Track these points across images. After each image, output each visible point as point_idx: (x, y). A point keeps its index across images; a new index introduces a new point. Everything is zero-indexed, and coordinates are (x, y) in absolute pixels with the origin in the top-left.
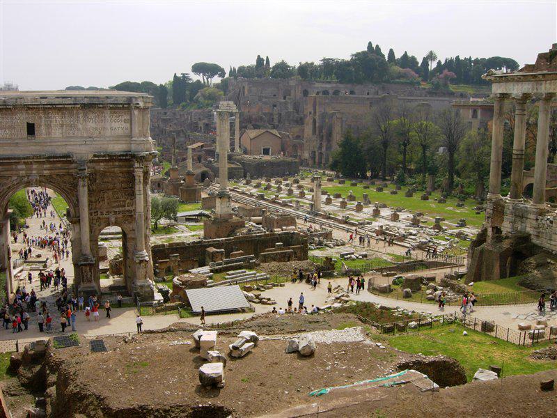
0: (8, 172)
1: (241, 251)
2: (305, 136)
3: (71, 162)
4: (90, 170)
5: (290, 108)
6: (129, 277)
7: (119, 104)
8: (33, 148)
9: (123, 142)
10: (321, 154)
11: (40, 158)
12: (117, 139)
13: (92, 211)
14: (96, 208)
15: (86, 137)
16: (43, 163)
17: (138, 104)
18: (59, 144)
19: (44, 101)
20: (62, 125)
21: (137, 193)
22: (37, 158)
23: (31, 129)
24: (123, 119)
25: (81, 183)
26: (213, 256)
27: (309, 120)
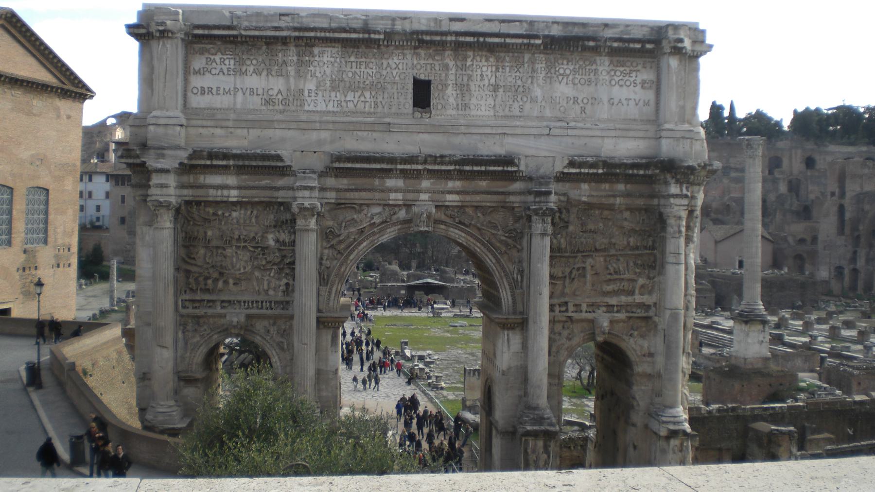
0: (364, 195)
2: (821, 237)
3: (511, 177)
4: (556, 197)
5: (783, 188)
9: (641, 134)
10: (855, 271)
11: (442, 163)
14: (563, 294)
15: (550, 119)
17: (681, 41)
18: (488, 130)
19: (457, 27)
20: (496, 88)
21: (670, 259)
22: (435, 163)
24: (639, 80)
25: (538, 226)
26: (770, 441)
27: (830, 206)
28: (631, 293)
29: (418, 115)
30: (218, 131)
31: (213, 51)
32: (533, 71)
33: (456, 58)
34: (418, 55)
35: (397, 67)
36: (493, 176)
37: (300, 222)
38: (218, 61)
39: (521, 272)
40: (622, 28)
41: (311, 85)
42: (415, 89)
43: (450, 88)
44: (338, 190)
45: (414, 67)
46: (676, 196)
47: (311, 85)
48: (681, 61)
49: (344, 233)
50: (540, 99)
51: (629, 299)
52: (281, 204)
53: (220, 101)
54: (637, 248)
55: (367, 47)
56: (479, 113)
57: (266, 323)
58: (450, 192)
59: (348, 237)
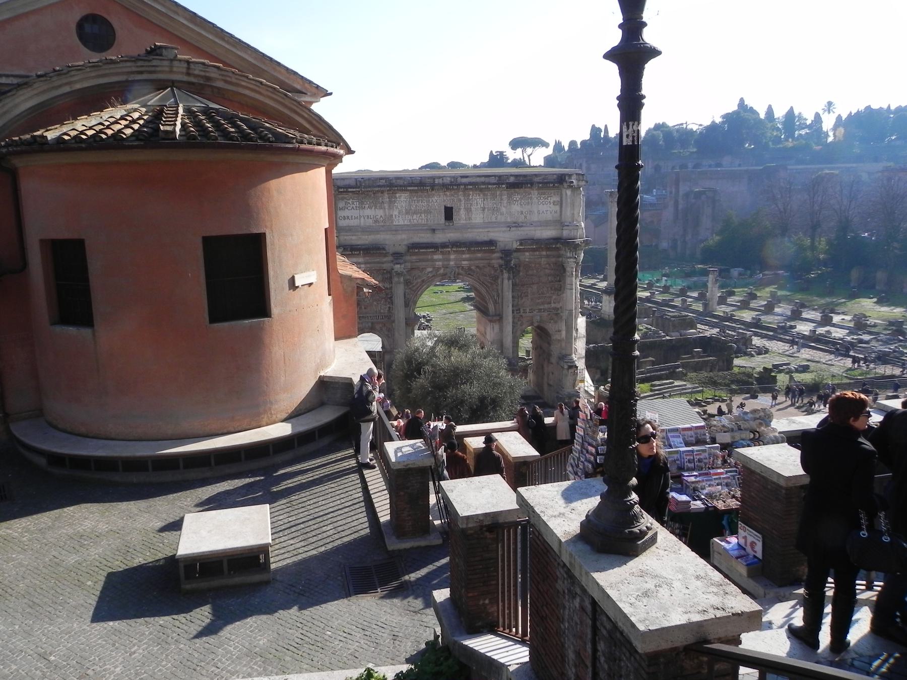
1: (651, 359)
3: (493, 252)
6: (549, 385)
7: (549, 183)
8: (452, 234)
12: (545, 224)
13: (515, 309)
16: (463, 253)
19: (464, 180)
20: (484, 209)
21: (568, 287)
23: (449, 213)
24: (552, 201)
28: (550, 303)
29: (447, 224)
30: (354, 238)
31: (348, 198)
32: (501, 199)
33: (464, 195)
34: (446, 195)
35: (436, 201)
36: (485, 252)
37: (395, 279)
38: (351, 203)
39: (498, 296)
40: (542, 177)
41: (396, 213)
42: (445, 212)
43: (462, 210)
44: (412, 262)
45: (444, 201)
46: (571, 258)
47: (396, 213)
48: (572, 191)
49: (415, 282)
50: (505, 213)
51: (549, 306)
52: (384, 270)
53: (353, 223)
54: (552, 282)
55: (422, 192)
56: (477, 222)
57: (381, 325)
58: (464, 260)
59: (417, 283)
